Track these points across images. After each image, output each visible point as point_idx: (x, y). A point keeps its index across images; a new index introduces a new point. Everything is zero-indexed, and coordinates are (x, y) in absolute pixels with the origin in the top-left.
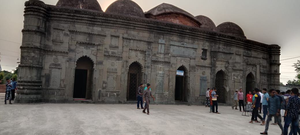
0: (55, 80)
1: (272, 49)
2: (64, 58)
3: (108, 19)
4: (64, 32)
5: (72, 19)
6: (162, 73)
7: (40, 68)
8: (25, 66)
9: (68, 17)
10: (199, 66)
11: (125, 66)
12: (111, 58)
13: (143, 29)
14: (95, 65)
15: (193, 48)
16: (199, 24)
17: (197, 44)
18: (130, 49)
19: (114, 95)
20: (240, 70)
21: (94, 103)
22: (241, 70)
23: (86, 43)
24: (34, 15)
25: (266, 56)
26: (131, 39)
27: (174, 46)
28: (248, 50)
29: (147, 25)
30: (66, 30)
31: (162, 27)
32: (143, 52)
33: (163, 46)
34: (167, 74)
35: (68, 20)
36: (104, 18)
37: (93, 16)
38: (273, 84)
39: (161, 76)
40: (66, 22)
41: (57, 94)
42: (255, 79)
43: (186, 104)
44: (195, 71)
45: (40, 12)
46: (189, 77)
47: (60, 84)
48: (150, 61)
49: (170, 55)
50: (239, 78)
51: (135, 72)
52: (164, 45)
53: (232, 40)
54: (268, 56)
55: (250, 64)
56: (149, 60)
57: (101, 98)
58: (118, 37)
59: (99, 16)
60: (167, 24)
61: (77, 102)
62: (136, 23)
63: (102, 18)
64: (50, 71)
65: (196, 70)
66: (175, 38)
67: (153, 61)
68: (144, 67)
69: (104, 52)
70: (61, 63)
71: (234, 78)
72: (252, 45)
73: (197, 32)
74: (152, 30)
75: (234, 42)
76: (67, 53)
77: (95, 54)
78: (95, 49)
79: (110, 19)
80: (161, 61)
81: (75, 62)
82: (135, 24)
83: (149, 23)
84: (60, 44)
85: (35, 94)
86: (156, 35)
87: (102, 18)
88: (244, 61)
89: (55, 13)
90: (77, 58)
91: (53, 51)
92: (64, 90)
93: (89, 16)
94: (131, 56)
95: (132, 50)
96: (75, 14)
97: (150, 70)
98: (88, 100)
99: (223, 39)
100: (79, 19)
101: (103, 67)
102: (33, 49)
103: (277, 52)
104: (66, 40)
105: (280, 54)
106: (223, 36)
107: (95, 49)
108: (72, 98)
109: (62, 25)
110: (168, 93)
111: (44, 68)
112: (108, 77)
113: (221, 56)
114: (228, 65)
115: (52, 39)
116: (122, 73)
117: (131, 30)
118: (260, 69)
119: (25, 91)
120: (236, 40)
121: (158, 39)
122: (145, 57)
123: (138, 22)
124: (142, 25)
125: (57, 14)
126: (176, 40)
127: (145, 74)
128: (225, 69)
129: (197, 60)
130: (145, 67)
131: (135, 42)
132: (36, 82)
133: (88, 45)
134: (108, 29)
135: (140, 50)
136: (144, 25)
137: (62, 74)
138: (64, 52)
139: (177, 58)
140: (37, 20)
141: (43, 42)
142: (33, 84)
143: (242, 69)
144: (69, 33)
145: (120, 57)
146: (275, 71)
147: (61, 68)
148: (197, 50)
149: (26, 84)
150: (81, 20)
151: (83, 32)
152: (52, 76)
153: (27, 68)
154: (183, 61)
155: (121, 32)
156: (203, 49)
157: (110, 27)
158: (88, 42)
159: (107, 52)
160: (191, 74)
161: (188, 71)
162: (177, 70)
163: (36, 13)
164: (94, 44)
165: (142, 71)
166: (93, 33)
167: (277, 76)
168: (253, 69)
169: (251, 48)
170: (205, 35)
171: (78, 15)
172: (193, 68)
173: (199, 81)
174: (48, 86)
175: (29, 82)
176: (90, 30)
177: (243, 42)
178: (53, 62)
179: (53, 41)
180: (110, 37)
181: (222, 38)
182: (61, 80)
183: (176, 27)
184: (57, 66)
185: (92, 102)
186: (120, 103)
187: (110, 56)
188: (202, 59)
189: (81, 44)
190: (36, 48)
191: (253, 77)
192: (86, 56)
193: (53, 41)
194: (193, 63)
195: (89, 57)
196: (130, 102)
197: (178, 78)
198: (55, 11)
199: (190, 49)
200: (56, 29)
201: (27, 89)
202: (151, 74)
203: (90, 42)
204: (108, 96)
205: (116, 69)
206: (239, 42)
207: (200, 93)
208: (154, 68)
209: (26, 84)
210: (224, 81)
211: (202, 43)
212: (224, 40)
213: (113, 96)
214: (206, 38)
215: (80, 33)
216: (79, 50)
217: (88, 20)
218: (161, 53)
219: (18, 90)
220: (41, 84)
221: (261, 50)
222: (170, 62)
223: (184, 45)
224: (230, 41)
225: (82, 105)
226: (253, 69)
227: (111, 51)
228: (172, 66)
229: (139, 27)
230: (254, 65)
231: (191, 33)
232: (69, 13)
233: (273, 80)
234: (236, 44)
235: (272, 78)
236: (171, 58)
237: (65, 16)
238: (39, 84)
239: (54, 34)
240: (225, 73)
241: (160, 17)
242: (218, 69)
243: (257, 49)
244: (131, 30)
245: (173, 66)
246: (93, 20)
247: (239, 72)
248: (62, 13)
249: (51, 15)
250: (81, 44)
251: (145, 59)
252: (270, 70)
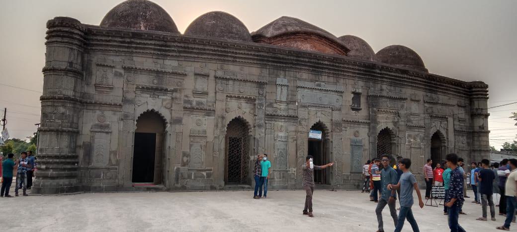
0: (101, 153)
1: (474, 90)
2: (114, 114)
3: (190, 46)
4: (114, 70)
5: (128, 47)
6: (284, 135)
7: (74, 132)
8: (48, 130)
9: (120, 44)
10: (347, 121)
11: (220, 125)
12: (195, 113)
13: (249, 61)
14: (168, 125)
15: (337, 91)
16: (346, 50)
17: (344, 84)
18: (227, 96)
19: (203, 176)
20: (420, 127)
21: (168, 190)
22: (421, 127)
23: (152, 89)
24: (63, 42)
25: (463, 101)
26: (229, 79)
27: (302, 90)
28: (431, 91)
29: (257, 53)
30: (118, 67)
31: (281, 56)
32: (250, 100)
33: (285, 90)
34: (293, 138)
35: (121, 49)
36: (183, 45)
37: (165, 41)
38: (479, 149)
39: (282, 141)
40: (117, 54)
41: (103, 175)
42: (446, 142)
43: (327, 189)
44: (341, 130)
45: (73, 38)
46: (332, 142)
47: (110, 160)
49: (297, 104)
50: (419, 140)
51: (238, 134)
52: (286, 88)
53: (403, 76)
54: (467, 102)
55: (436, 117)
56: (261, 115)
57: (179, 181)
58: (206, 76)
59: (173, 42)
60: (290, 52)
61: (138, 190)
62: (238, 51)
63: (179, 45)
64: (93, 138)
65: (343, 129)
66: (305, 75)
67: (268, 115)
68: (252, 126)
69: (183, 102)
70: (110, 123)
71: (410, 142)
72: (439, 83)
73: (343, 64)
74: (265, 63)
75: (407, 78)
76: (120, 105)
77: (169, 106)
78: (168, 97)
79: (193, 46)
80: (281, 116)
81: (134, 121)
82: (236, 53)
83: (259, 51)
84: (108, 90)
85: (68, 177)
86: (272, 70)
87: (179, 45)
88: (426, 111)
89: (99, 38)
90: (138, 114)
91: (95, 103)
92: (116, 169)
93: (157, 43)
94: (229, 108)
95: (231, 97)
96: (132, 40)
97: (264, 131)
98: (157, 186)
99: (387, 74)
100: (141, 48)
101: (182, 128)
102: (61, 101)
103: (482, 95)
104: (118, 83)
105: (488, 98)
106: (387, 69)
107: (168, 98)
108: (129, 183)
109: (111, 58)
110: (295, 169)
111: (81, 133)
112: (191, 146)
113: (386, 104)
114: (398, 119)
115: (93, 82)
116: (215, 137)
117: (230, 63)
118: (454, 125)
119: (50, 172)
120: (410, 75)
121: (276, 78)
122: (254, 109)
123: (240, 49)
124: (248, 54)
125: (102, 40)
126: (307, 78)
127: (254, 138)
128: (393, 126)
129: (343, 111)
130: (254, 127)
131: (237, 83)
132: (68, 157)
133: (155, 91)
134: (190, 63)
135: (245, 96)
136: (251, 55)
137: (113, 142)
138: (115, 105)
139: (309, 108)
140: (67, 51)
141: (78, 88)
142: (63, 160)
143: (423, 125)
144: (122, 71)
145: (210, 110)
146: (480, 127)
147: (111, 133)
148: (344, 95)
149: (51, 160)
150: (144, 49)
151: (147, 70)
152: (96, 146)
153: (53, 133)
154: (319, 114)
155: (212, 68)
156: (353, 93)
157: (193, 60)
158: (155, 85)
160: (334, 137)
161: (330, 131)
162: (311, 129)
163: (66, 40)
164: (166, 90)
165: (250, 134)
166: (163, 70)
167: (484, 136)
168: (442, 125)
169: (437, 88)
170: (357, 68)
171: (138, 41)
172: (337, 125)
173: (349, 147)
174: (89, 163)
175: (56, 157)
176: (159, 66)
177: (423, 78)
178: (97, 122)
179: (96, 86)
180: (193, 77)
181: (385, 73)
182: (111, 152)
183: (305, 56)
184: (103, 128)
185: (166, 188)
186: (213, 188)
187: (194, 109)
188: (353, 109)
189: (145, 89)
190: (67, 98)
191: (442, 139)
192: (153, 111)
193: (96, 86)
194: (337, 116)
195: (158, 112)
196: (230, 187)
197: (312, 143)
198: (98, 35)
199: (331, 93)
200: (101, 65)
201: (51, 169)
202: (265, 138)
203: (160, 86)
204: (193, 178)
205: (205, 132)
206: (416, 78)
207: (352, 170)
208: (270, 128)
209: (51, 160)
210: (393, 147)
211: (350, 82)
212: (390, 75)
213: (201, 177)
214: (358, 74)
215: (142, 71)
216: (140, 101)
217: (154, 49)
218: (281, 102)
219: (39, 172)
220: (77, 160)
221: (455, 92)
222: (297, 117)
223: (320, 86)
224: (400, 77)
225: (148, 194)
226: (442, 125)
227: (195, 100)
228: (300, 124)
229: (242, 58)
230: (444, 118)
231: (333, 66)
232: (122, 37)
233: (477, 143)
234: (411, 82)
235: (476, 138)
236: (299, 109)
237: (115, 44)
238: (73, 160)
239: (97, 75)
240: (393, 132)
241: (278, 39)
242: (381, 127)
243: (447, 90)
244: (228, 63)
245: (303, 122)
246: (164, 48)
247: (417, 130)
248: (110, 38)
249: (92, 42)
250: (145, 89)
251: (255, 112)
252: (472, 126)
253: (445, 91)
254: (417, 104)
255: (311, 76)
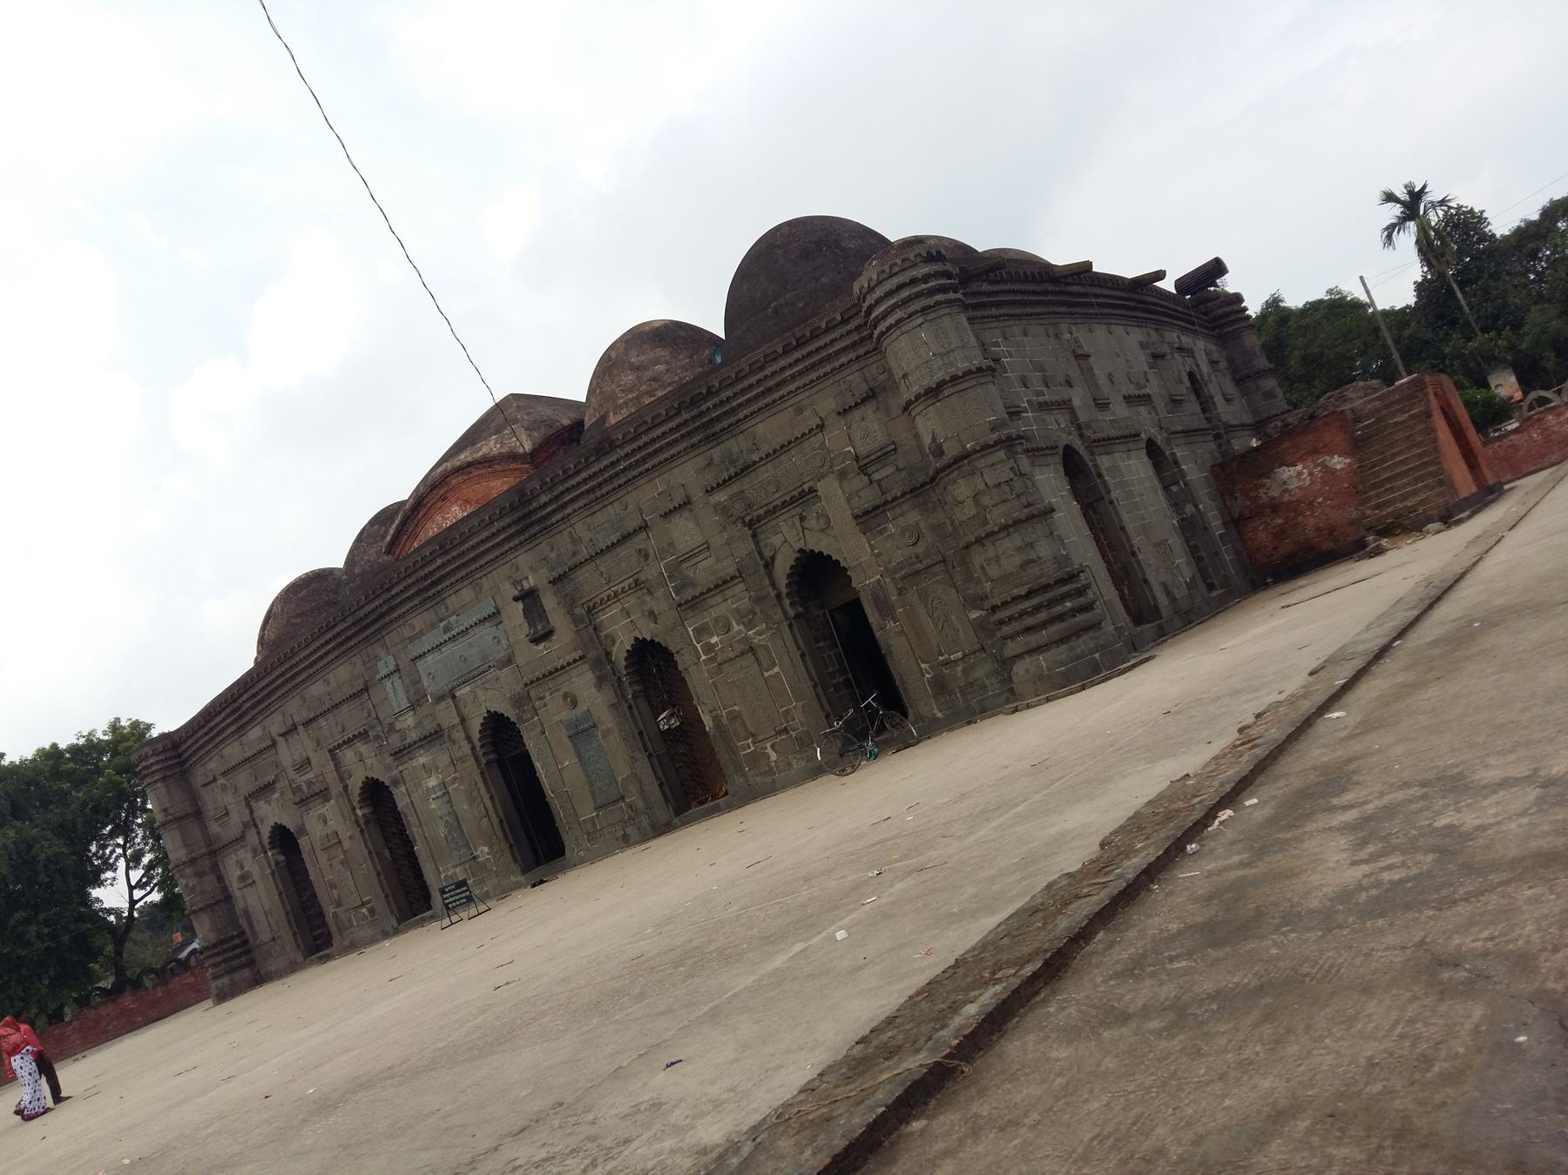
18: (330, 751)
28: (713, 438)
32: (363, 736)
48: (390, 760)
50: (736, 627)
52: (395, 678)
53: (614, 458)
66: (418, 621)
71: (709, 648)
129: (520, 660)
143: (732, 570)
148: (504, 616)
156: (516, 599)
159: (298, 789)
172: (519, 701)
218: (401, 713)
227: (302, 780)
247: (719, 598)
253: (768, 400)
254: (686, 514)
255: (429, 616)
